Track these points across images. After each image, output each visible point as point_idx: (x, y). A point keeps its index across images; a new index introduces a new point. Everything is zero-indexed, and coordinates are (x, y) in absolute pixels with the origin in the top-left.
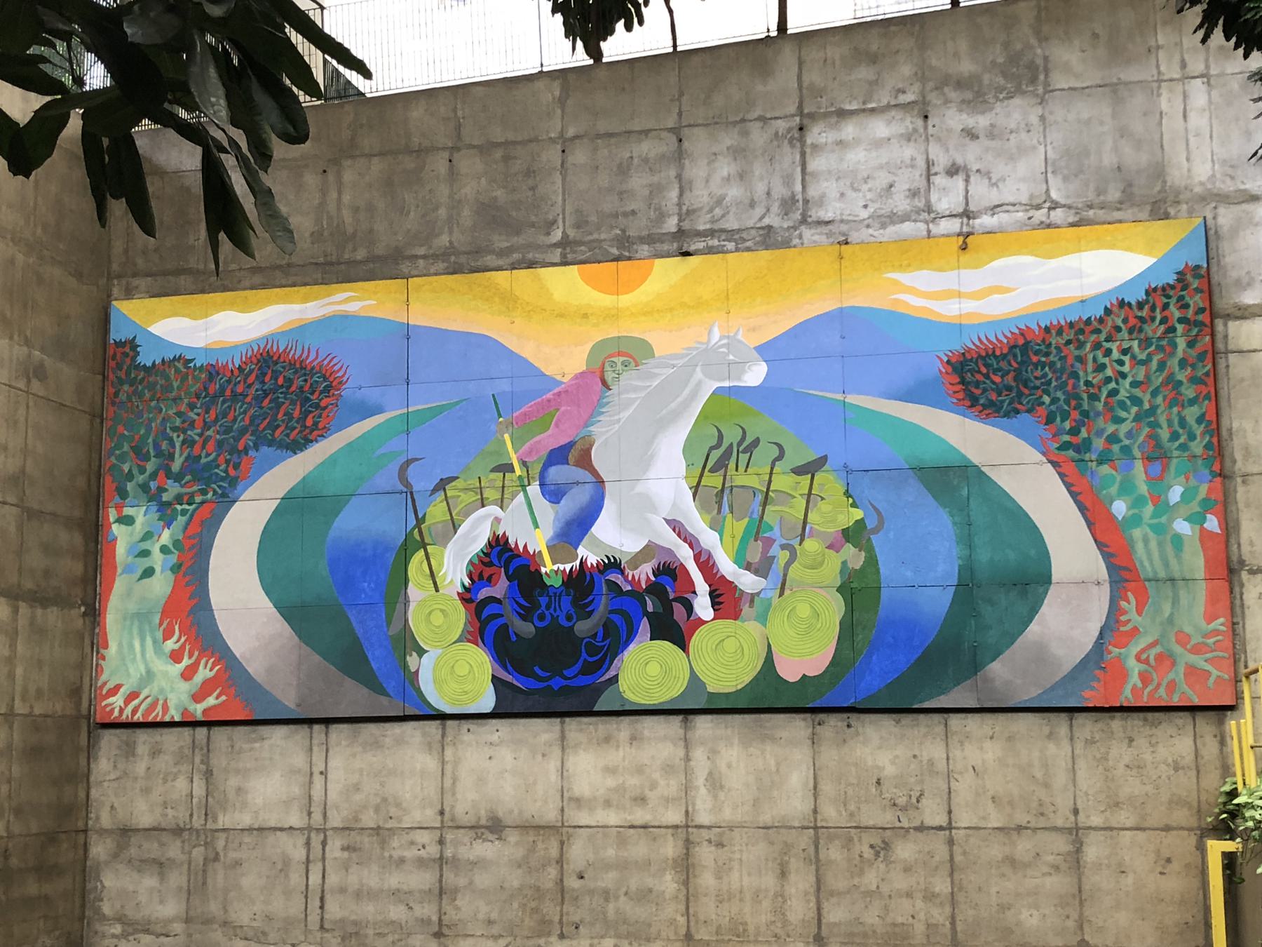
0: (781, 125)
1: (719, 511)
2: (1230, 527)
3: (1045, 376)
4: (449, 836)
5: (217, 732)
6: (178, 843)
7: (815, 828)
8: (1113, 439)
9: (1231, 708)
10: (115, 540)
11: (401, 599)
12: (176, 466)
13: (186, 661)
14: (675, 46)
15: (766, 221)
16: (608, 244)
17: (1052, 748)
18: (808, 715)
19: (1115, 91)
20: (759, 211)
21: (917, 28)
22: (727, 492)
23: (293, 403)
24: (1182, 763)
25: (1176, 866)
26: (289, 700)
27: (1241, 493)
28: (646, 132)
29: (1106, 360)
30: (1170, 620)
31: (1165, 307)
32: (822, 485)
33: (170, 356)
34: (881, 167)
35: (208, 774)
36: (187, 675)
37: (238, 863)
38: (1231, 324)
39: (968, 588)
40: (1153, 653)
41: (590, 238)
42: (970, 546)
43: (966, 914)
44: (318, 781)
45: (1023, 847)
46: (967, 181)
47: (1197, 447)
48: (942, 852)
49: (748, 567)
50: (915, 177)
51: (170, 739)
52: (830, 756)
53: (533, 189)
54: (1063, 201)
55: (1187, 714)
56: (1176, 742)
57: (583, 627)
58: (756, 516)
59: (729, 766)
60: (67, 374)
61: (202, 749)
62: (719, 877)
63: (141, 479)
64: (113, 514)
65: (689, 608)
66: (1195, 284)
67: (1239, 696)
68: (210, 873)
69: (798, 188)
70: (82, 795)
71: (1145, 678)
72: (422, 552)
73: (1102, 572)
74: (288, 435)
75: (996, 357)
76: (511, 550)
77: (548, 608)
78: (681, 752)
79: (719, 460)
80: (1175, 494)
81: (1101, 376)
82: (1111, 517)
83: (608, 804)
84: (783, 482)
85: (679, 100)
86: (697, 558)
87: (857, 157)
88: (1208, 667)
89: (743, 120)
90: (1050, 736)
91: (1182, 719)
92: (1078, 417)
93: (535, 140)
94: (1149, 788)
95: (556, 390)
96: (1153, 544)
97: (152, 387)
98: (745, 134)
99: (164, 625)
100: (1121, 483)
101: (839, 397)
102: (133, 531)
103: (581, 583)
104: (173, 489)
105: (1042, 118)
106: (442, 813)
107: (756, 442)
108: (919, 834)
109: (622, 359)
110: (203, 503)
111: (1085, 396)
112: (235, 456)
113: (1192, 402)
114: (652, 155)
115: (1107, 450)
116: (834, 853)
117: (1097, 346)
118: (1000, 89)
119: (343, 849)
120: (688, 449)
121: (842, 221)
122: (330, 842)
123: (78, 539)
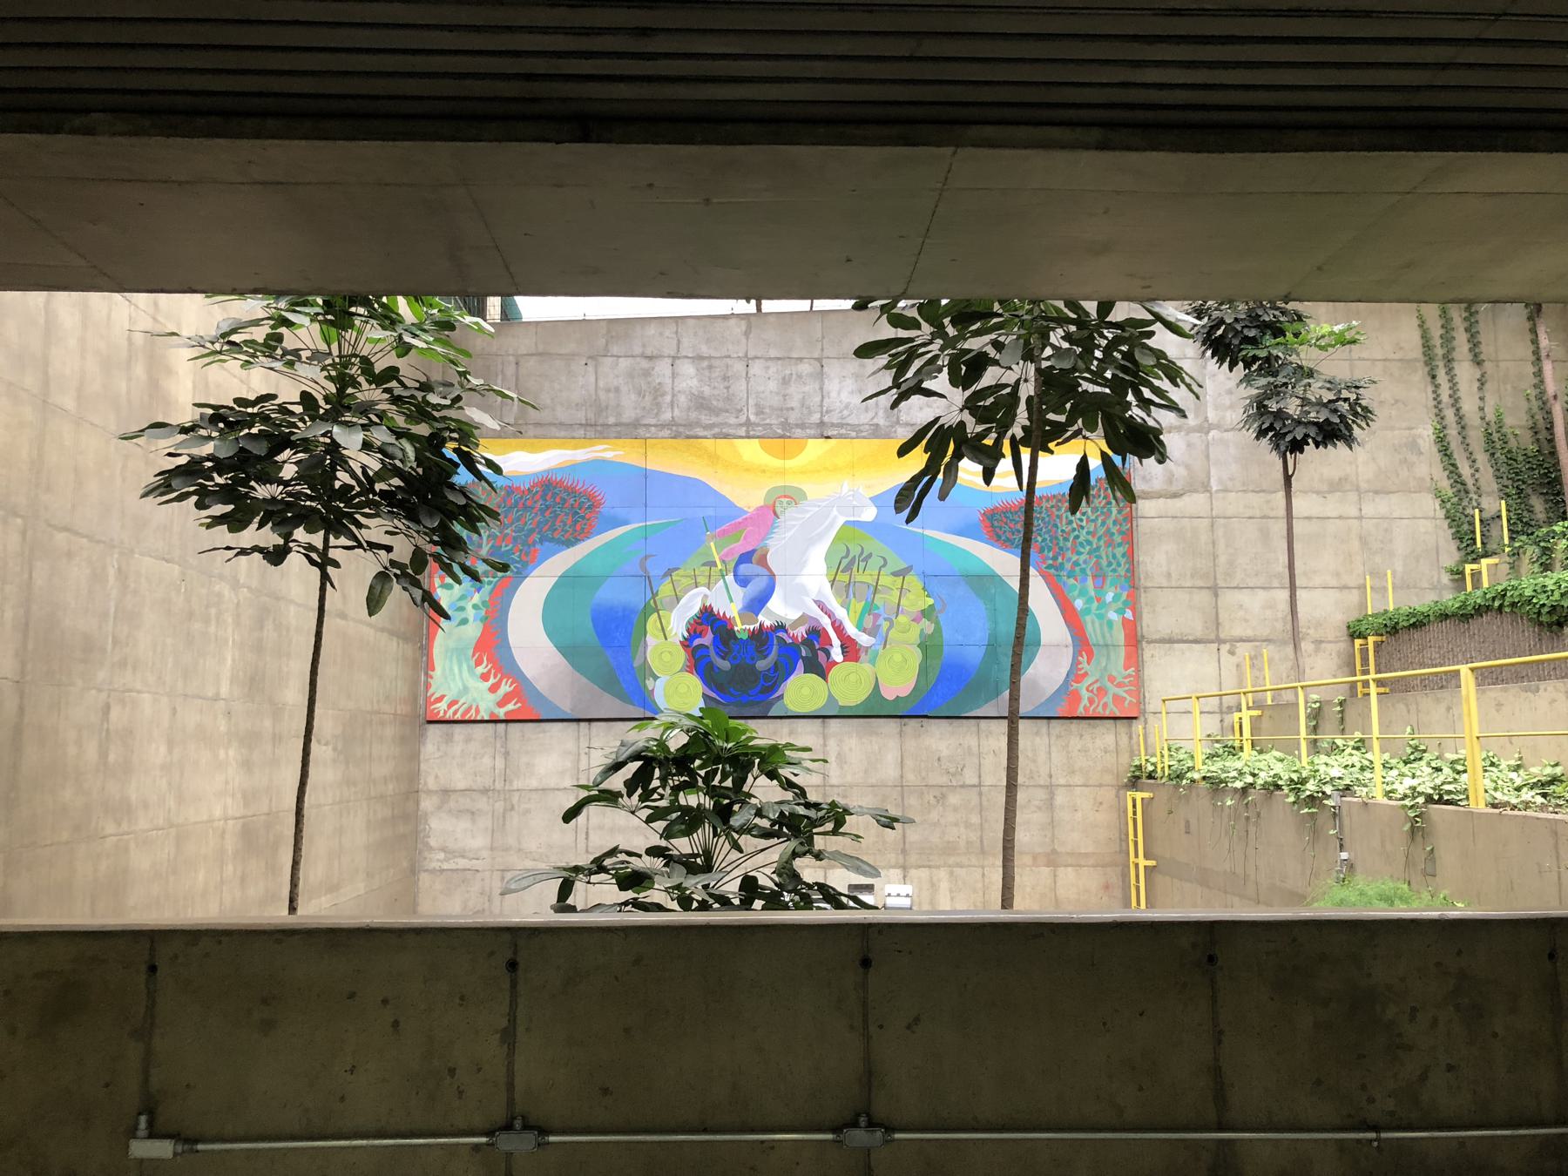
5: (511, 725)
8: (1076, 563)
13: (492, 681)
20: (871, 414)
26: (567, 708)
27: (1143, 598)
28: (801, 359)
35: (507, 754)
36: (493, 689)
37: (528, 811)
42: (996, 623)
47: (1122, 571)
49: (864, 631)
52: (911, 744)
56: (1105, 737)
65: (828, 654)
71: (1091, 701)
80: (1109, 596)
82: (1074, 609)
84: (886, 580)
86: (833, 624)
90: (1037, 733)
103: (762, 638)
107: (870, 555)
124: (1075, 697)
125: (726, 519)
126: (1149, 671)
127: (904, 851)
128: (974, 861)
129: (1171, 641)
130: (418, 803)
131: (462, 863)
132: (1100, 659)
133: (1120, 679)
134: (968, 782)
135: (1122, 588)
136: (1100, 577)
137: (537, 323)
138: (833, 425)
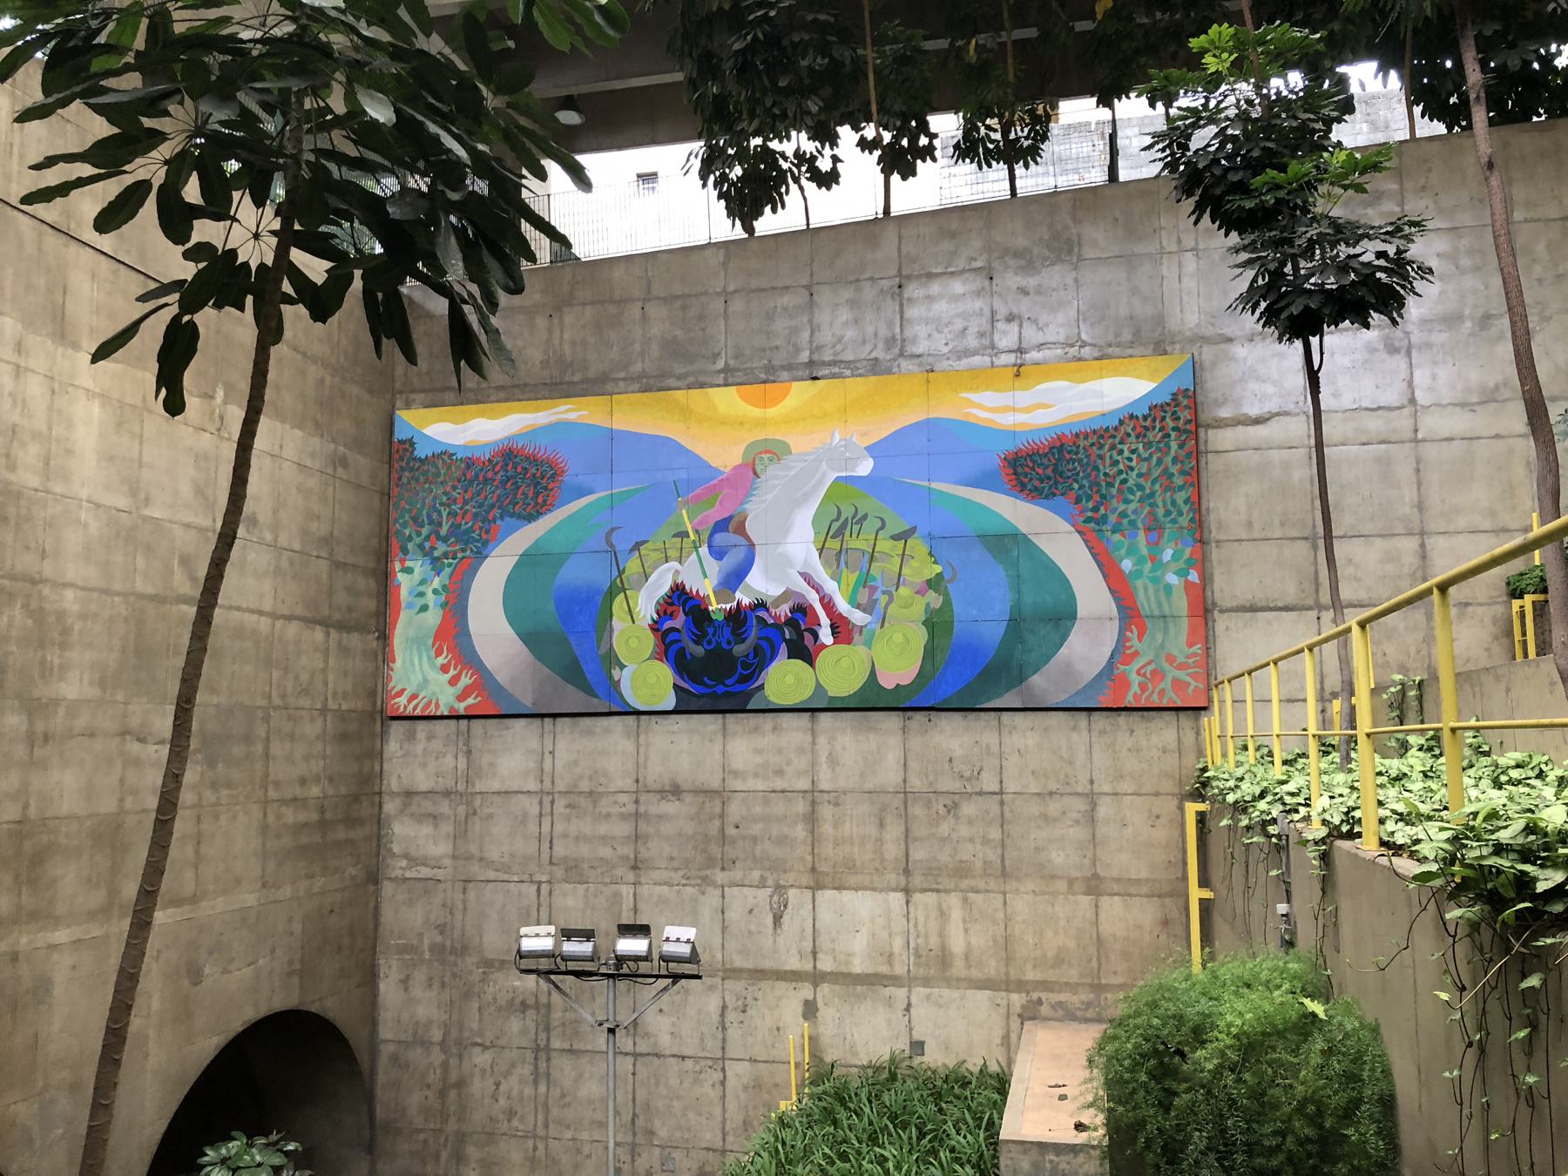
0: (885, 284)
2: (1206, 578)
4: (643, 798)
5: (474, 722)
7: (905, 793)
8: (1123, 514)
9: (1204, 709)
12: (444, 531)
13: (452, 672)
15: (874, 355)
16: (760, 371)
17: (1075, 736)
19: (1129, 261)
20: (868, 347)
25: (1163, 820)
26: (527, 702)
27: (1215, 554)
28: (786, 288)
30: (1162, 646)
31: (1163, 419)
34: (958, 315)
36: (453, 682)
37: (490, 817)
38: (1210, 432)
39: (1016, 623)
43: (1011, 854)
45: (1054, 807)
46: (1021, 326)
47: (1184, 521)
48: (995, 809)
49: (858, 607)
50: (983, 323)
52: (915, 742)
56: (1164, 732)
57: (739, 649)
59: (844, 749)
60: (363, 463)
62: (835, 826)
63: (418, 540)
64: (398, 566)
65: (816, 636)
67: (1210, 700)
69: (898, 330)
70: (377, 768)
71: (1143, 687)
78: (809, 739)
79: (837, 530)
80: (1168, 555)
82: (1120, 571)
83: (756, 775)
84: (884, 545)
86: (821, 600)
87: (941, 308)
88: (1188, 679)
90: (1074, 728)
91: (1167, 715)
93: (706, 293)
96: (1151, 591)
98: (859, 290)
101: (925, 483)
102: (414, 579)
103: (738, 617)
104: (441, 548)
105: (1076, 280)
106: (637, 781)
107: (865, 517)
113: (1181, 488)
115: (1119, 522)
116: (917, 810)
117: (1113, 447)
118: (1045, 259)
120: (816, 521)
123: (372, 584)
124: (1124, 683)
125: (700, 483)
127: (907, 872)
128: (993, 885)
129: (1253, 609)
131: (425, 872)
132: (1155, 634)
133: (1181, 659)
134: (986, 789)
136: (1154, 528)
138: (824, 364)
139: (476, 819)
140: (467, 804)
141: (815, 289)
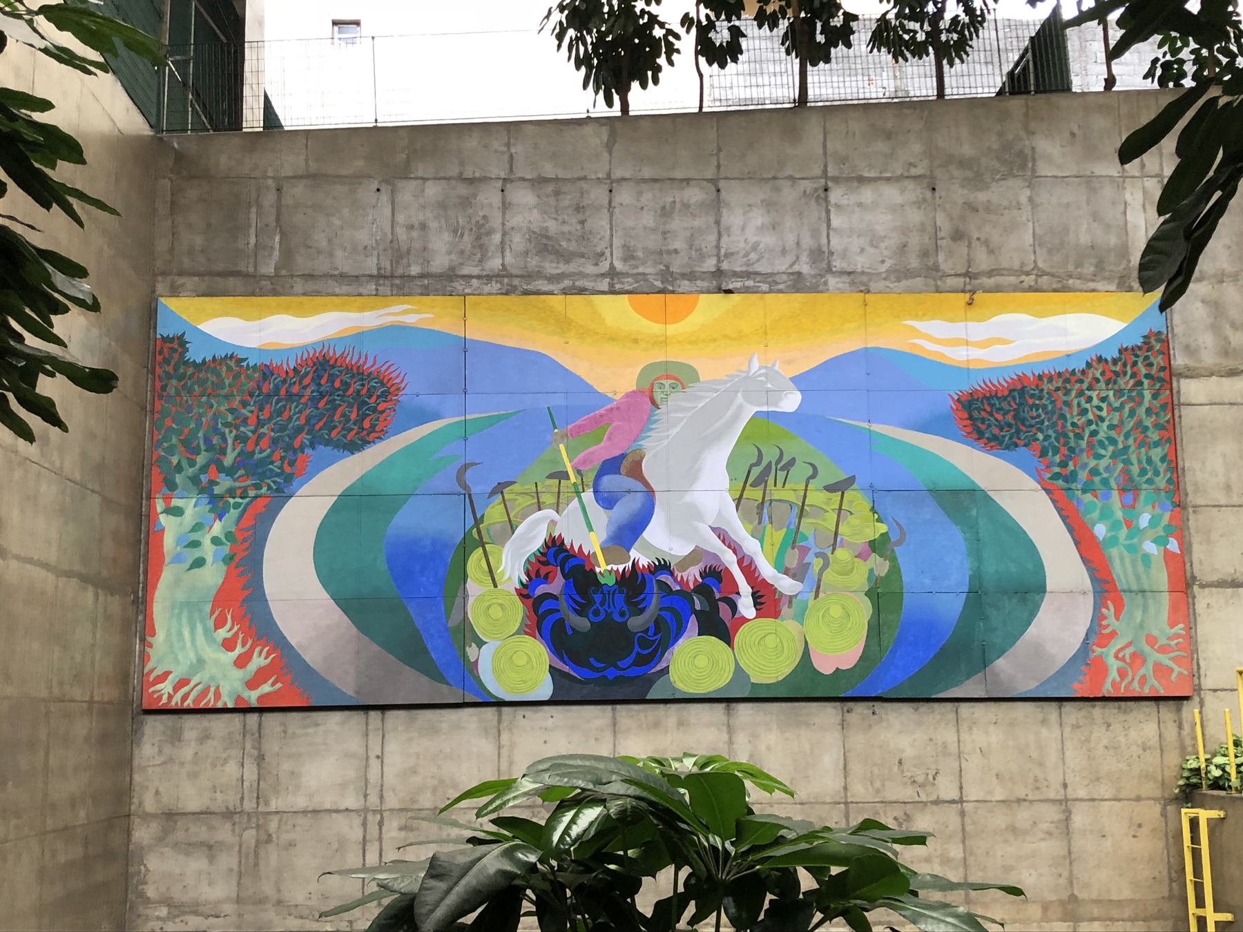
0: (808, 185)
1: (760, 523)
2: (1186, 546)
3: (1039, 416)
5: (269, 718)
6: (228, 826)
8: (1094, 472)
9: (1187, 698)
10: (163, 530)
11: (460, 593)
12: (229, 460)
13: (239, 650)
14: (701, 107)
15: (796, 268)
17: (1044, 732)
18: (838, 704)
20: (790, 258)
21: (926, 113)
22: (766, 504)
23: (350, 405)
24: (1151, 743)
25: (1145, 830)
26: (349, 690)
28: (687, 181)
29: (1088, 406)
30: (1141, 626)
31: (1135, 364)
32: (851, 502)
33: (221, 353)
35: (260, 759)
36: (241, 662)
37: (292, 844)
38: (1183, 381)
39: (977, 596)
40: (1128, 651)
41: (635, 271)
42: (979, 559)
44: (375, 765)
45: (1023, 816)
46: (969, 246)
47: (1161, 482)
48: (954, 821)
49: (786, 572)
51: (219, 724)
52: (858, 740)
53: (582, 222)
54: (1048, 270)
55: (1153, 703)
56: (1144, 726)
57: (636, 623)
58: (793, 527)
59: (769, 748)
61: (253, 734)
64: (160, 505)
65: (734, 607)
66: (1158, 346)
68: (262, 854)
69: (824, 241)
70: (128, 779)
71: (1122, 673)
72: (480, 550)
73: (1087, 583)
74: (345, 436)
75: (998, 398)
76: (566, 550)
77: (602, 604)
78: (725, 737)
79: (757, 476)
80: (1144, 520)
81: (1083, 419)
82: (1093, 537)
84: (816, 497)
85: (717, 154)
86: (740, 562)
88: (1172, 664)
89: (775, 178)
90: (1044, 722)
91: (1149, 707)
92: (1067, 452)
93: (585, 178)
94: (1122, 766)
95: (609, 407)
96: (1127, 561)
97: (202, 383)
98: (777, 190)
99: (217, 613)
100: (1102, 510)
101: (865, 425)
102: (181, 521)
103: (633, 582)
104: (224, 483)
105: (1030, 199)
108: (935, 808)
109: (670, 381)
110: (256, 497)
111: (1071, 435)
112: (291, 452)
113: (1156, 444)
114: (693, 201)
115: (1090, 481)
117: (1080, 393)
119: (400, 829)
120: (731, 465)
121: (863, 273)
122: (386, 823)
124: (1100, 668)
126: (1205, 628)
130: (129, 833)
133: (1163, 641)
135: (1163, 508)
137: (308, 135)
138: (735, 274)
139: (271, 848)
140: (258, 827)
141: (722, 184)
